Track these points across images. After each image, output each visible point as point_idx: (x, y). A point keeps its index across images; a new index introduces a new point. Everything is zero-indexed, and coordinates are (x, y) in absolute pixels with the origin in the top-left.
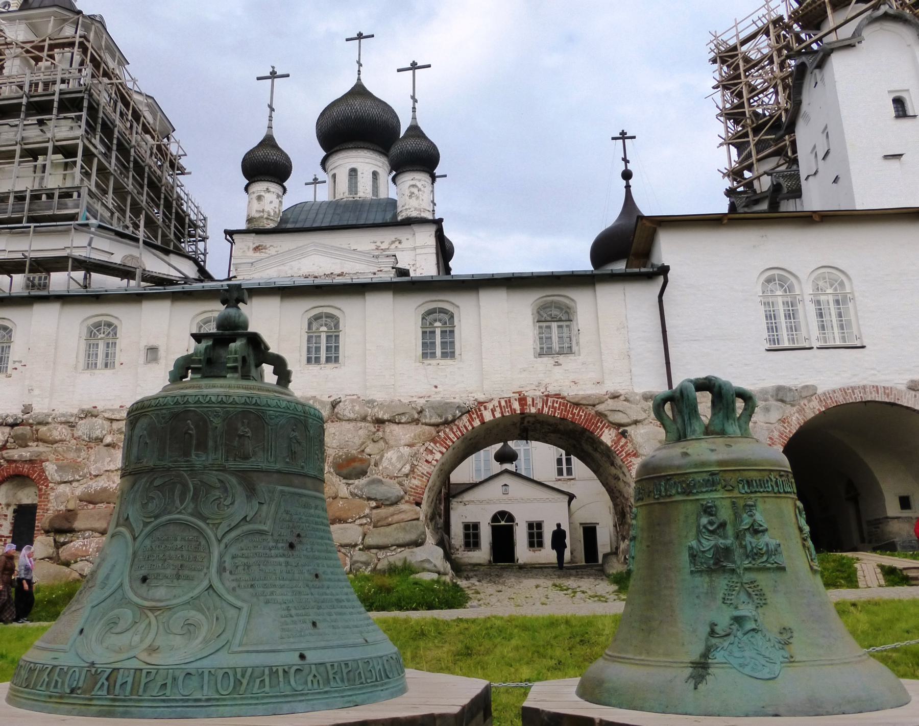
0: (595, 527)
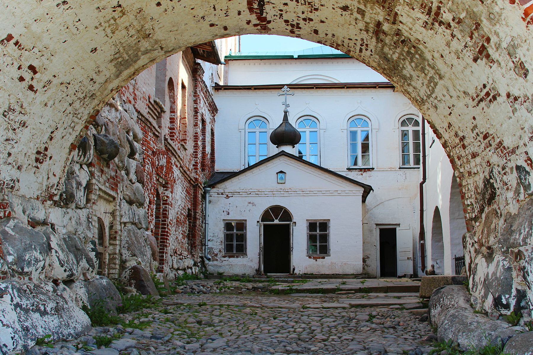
0: (395, 229)
